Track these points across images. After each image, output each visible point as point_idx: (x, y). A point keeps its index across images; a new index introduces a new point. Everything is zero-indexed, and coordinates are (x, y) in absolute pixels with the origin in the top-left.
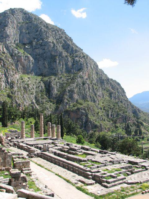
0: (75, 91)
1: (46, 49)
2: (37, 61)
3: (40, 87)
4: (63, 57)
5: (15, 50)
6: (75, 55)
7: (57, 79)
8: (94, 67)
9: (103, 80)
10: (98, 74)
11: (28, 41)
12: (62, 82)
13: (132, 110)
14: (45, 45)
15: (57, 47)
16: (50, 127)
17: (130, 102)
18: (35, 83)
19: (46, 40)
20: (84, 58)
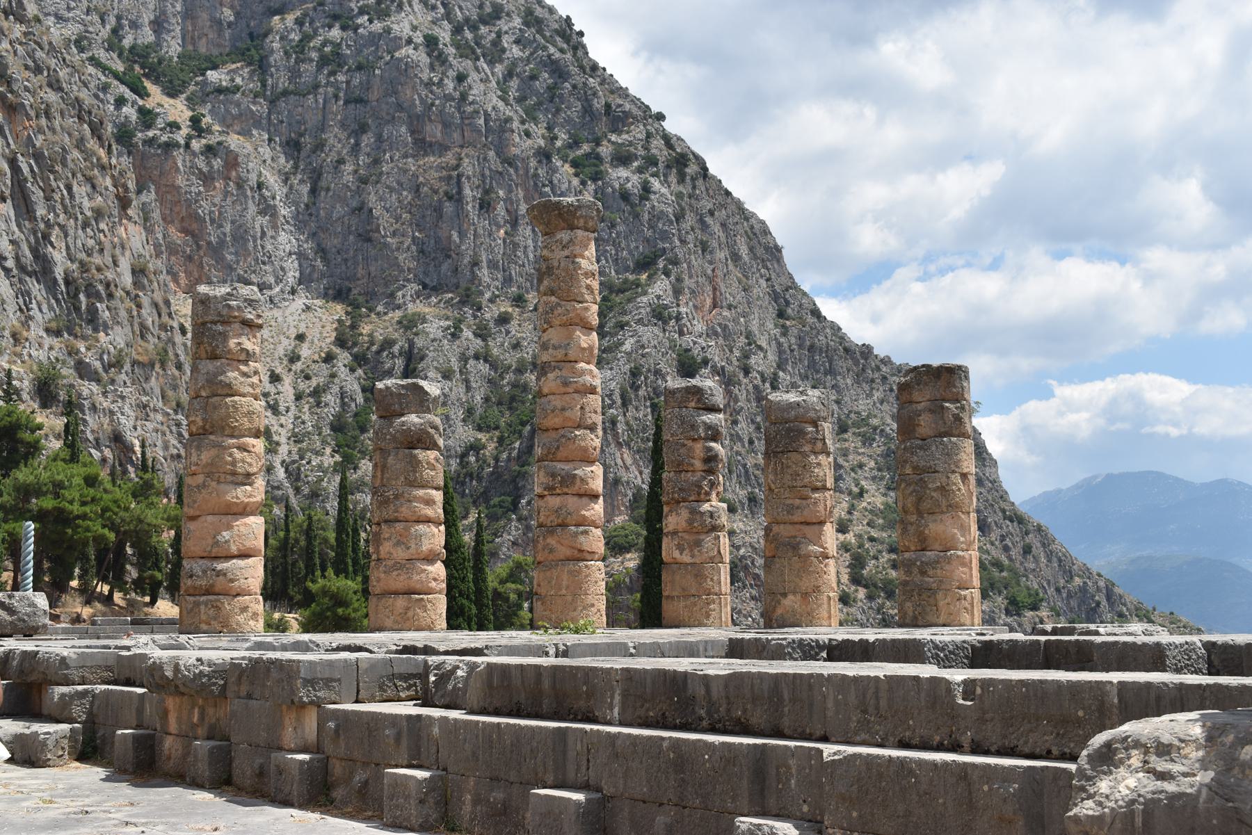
0: (621, 427)
1: (373, 96)
2: (305, 189)
3: (330, 398)
4: (509, 162)
5: (120, 102)
6: (605, 150)
7: (467, 333)
8: (751, 249)
9: (828, 352)
10: (787, 303)
11: (227, 33)
12: (511, 359)
13: (1058, 590)
14: (360, 68)
15: (461, 78)
16: (711, 459)
17: (1039, 529)
18: (294, 358)
19: (377, 26)
20: (682, 179)
